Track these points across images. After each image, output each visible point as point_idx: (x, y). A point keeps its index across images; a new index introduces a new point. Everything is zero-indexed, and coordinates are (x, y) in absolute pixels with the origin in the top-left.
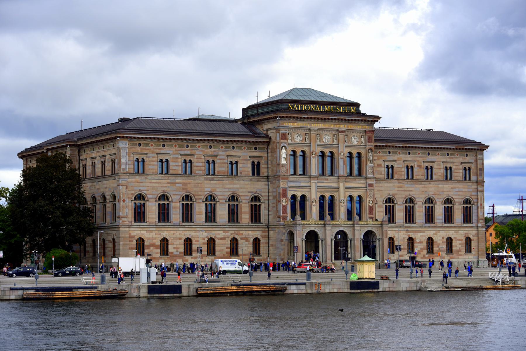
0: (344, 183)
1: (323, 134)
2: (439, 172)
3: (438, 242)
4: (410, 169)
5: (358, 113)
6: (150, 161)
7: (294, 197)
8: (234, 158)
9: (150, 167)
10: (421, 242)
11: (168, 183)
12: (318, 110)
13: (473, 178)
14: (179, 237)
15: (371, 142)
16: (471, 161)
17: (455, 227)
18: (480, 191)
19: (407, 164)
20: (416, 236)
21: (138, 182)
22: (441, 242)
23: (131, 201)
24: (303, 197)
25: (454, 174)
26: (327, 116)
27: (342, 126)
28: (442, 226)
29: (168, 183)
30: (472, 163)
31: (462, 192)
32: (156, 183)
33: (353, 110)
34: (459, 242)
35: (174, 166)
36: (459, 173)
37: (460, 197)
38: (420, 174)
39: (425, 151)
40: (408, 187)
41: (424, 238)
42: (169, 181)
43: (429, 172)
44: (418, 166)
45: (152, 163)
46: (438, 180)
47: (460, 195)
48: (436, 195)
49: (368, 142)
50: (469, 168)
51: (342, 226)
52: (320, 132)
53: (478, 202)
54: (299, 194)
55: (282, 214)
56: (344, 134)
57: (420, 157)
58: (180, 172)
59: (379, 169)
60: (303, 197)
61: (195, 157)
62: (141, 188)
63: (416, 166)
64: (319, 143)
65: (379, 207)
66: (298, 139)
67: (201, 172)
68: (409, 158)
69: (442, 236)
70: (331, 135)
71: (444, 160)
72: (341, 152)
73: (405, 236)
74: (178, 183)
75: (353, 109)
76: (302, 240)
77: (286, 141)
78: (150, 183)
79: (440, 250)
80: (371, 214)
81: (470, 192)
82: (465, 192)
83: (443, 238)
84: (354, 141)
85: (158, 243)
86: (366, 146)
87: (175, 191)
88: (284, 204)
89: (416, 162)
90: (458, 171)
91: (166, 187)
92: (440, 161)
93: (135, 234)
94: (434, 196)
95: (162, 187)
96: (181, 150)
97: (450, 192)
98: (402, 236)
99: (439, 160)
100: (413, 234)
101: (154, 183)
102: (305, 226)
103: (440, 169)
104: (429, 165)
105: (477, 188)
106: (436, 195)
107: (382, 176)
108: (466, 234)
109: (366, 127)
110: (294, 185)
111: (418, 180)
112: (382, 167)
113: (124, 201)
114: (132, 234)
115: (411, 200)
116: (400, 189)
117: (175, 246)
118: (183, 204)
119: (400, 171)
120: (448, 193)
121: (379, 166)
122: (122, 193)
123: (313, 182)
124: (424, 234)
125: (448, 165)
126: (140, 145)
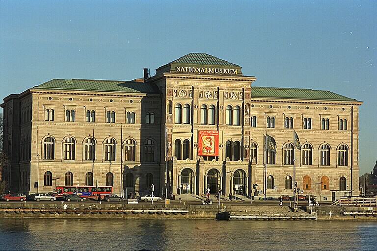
2: (316, 123)
5: (240, 75)
7: (178, 142)
11: (73, 129)
12: (202, 71)
14: (81, 171)
17: (331, 168)
19: (287, 115)
24: (187, 141)
25: (330, 125)
29: (73, 129)
30: (348, 116)
33: (236, 72)
34: (333, 181)
39: (305, 106)
45: (60, 113)
50: (346, 120)
54: (182, 139)
56: (224, 91)
57: (299, 110)
59: (261, 119)
62: (51, 133)
63: (295, 118)
67: (102, 120)
68: (288, 111)
75: (235, 70)
76: (179, 176)
85: (63, 175)
89: (295, 115)
90: (335, 122)
97: (327, 139)
99: (317, 113)
104: (308, 117)
109: (245, 85)
115: (328, 147)
116: (279, 136)
117: (78, 178)
120: (324, 140)
122: (34, 136)
125: (326, 117)
126: (50, 98)
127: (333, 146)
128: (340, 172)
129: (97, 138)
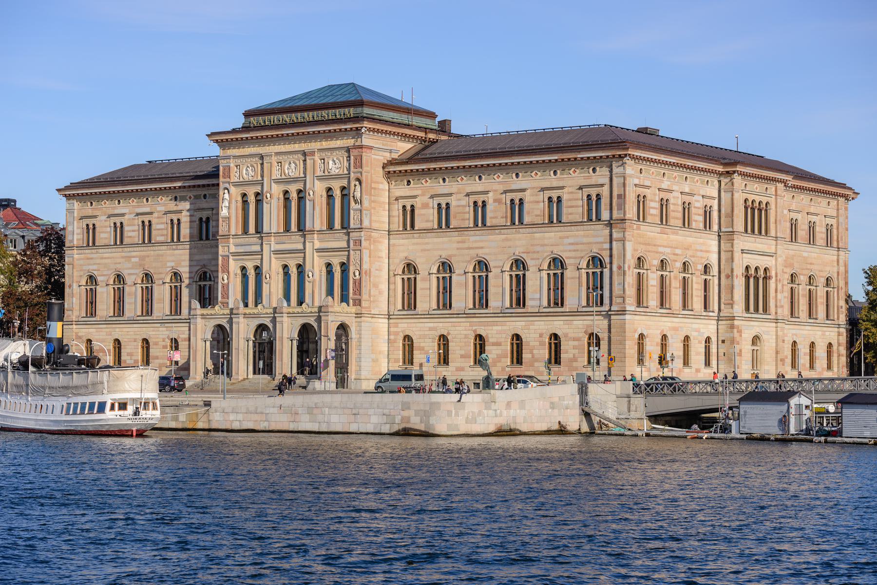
2: (535, 209)
3: (531, 344)
4: (480, 208)
6: (102, 227)
8: (205, 212)
9: (103, 235)
10: (498, 344)
11: (123, 257)
13: (605, 215)
16: (601, 181)
17: (563, 314)
18: (618, 240)
19: (473, 198)
20: (489, 332)
21: (88, 259)
22: (538, 343)
23: (80, 286)
25: (565, 210)
28: (539, 312)
29: (123, 257)
30: (602, 185)
31: (583, 244)
32: (108, 258)
34: (572, 343)
35: (130, 231)
36: (577, 206)
37: (579, 254)
38: (500, 214)
40: (476, 241)
41: (504, 336)
42: (124, 254)
43: (517, 208)
44: (495, 201)
45: (104, 229)
46: (533, 225)
47: (578, 250)
48: (529, 253)
50: (598, 196)
53: (611, 263)
58: (136, 241)
59: (423, 211)
61: (155, 215)
62: (91, 267)
64: (279, 177)
65: (423, 280)
69: (539, 331)
71: (547, 184)
73: (469, 332)
74: (134, 257)
77: (228, 180)
78: (102, 258)
79: (534, 359)
80: (356, 294)
81: (597, 243)
82: (588, 244)
83: (541, 335)
84: (334, 168)
86: (349, 174)
87: (130, 269)
89: (491, 195)
90: (574, 203)
91: (120, 263)
92: (537, 188)
93: (84, 334)
94: (524, 256)
95: (115, 263)
96: (138, 207)
98: (462, 332)
100: (483, 327)
101: (105, 258)
103: (538, 202)
104: (517, 196)
105: (611, 235)
106: (529, 253)
107: (429, 225)
108: (588, 326)
110: (242, 251)
111: (494, 227)
112: (430, 208)
113: (70, 286)
114: (80, 334)
116: (461, 245)
117: (129, 351)
118: (200, 285)
119: (460, 213)
120: (551, 248)
121: (425, 206)
124: (504, 328)
125: (554, 194)
127: (571, 261)
128: (586, 322)
129: (155, 273)
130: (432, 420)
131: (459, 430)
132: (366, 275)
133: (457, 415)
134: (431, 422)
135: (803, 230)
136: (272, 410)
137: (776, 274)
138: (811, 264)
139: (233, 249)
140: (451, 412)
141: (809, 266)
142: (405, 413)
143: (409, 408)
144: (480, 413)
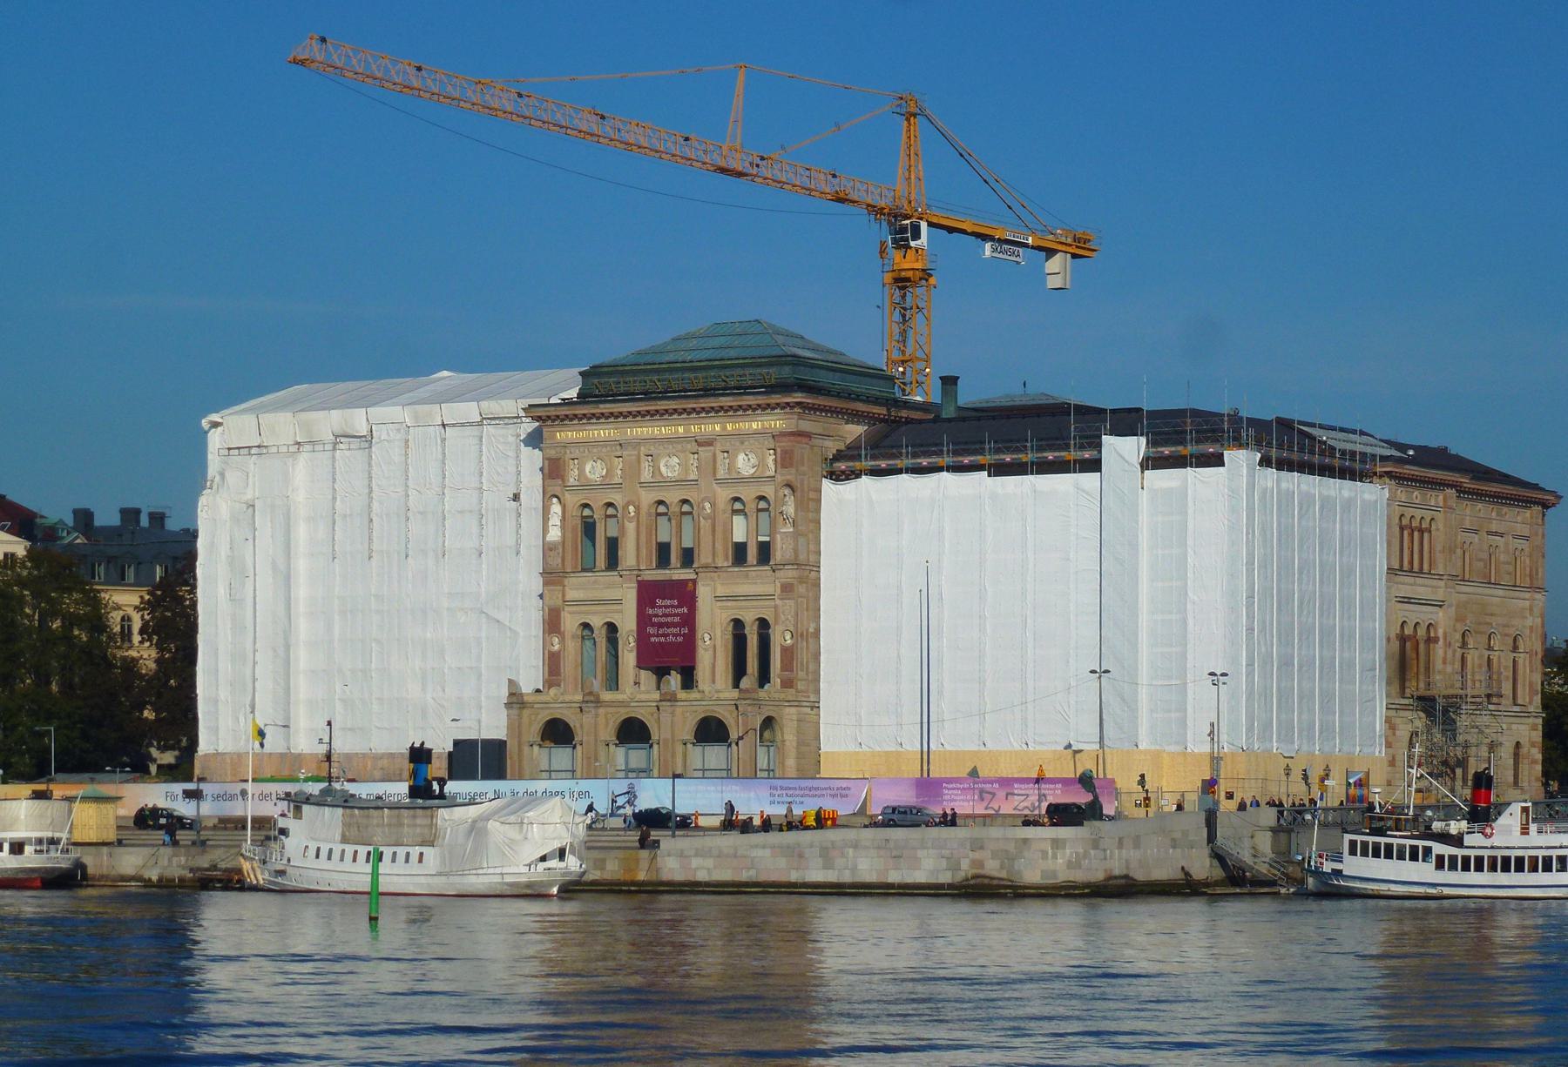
0: (708, 585)
1: (659, 455)
15: (791, 465)
26: (651, 405)
27: (709, 428)
49: (784, 466)
51: (632, 704)
52: (653, 450)
54: (597, 622)
55: (549, 675)
60: (612, 628)
66: (594, 470)
70: (682, 455)
72: (703, 500)
80: (787, 671)
84: (745, 464)
88: (556, 647)
102: (536, 706)
123: (628, 588)
130: (1020, 864)
131: (1055, 877)
132: (802, 639)
133: (1055, 857)
134: (1016, 867)
135: (1480, 560)
136: (759, 853)
137: (1445, 634)
138: (1492, 615)
139: (572, 594)
140: (1047, 853)
141: (1488, 619)
142: (977, 855)
143: (982, 848)
144: (1086, 855)
